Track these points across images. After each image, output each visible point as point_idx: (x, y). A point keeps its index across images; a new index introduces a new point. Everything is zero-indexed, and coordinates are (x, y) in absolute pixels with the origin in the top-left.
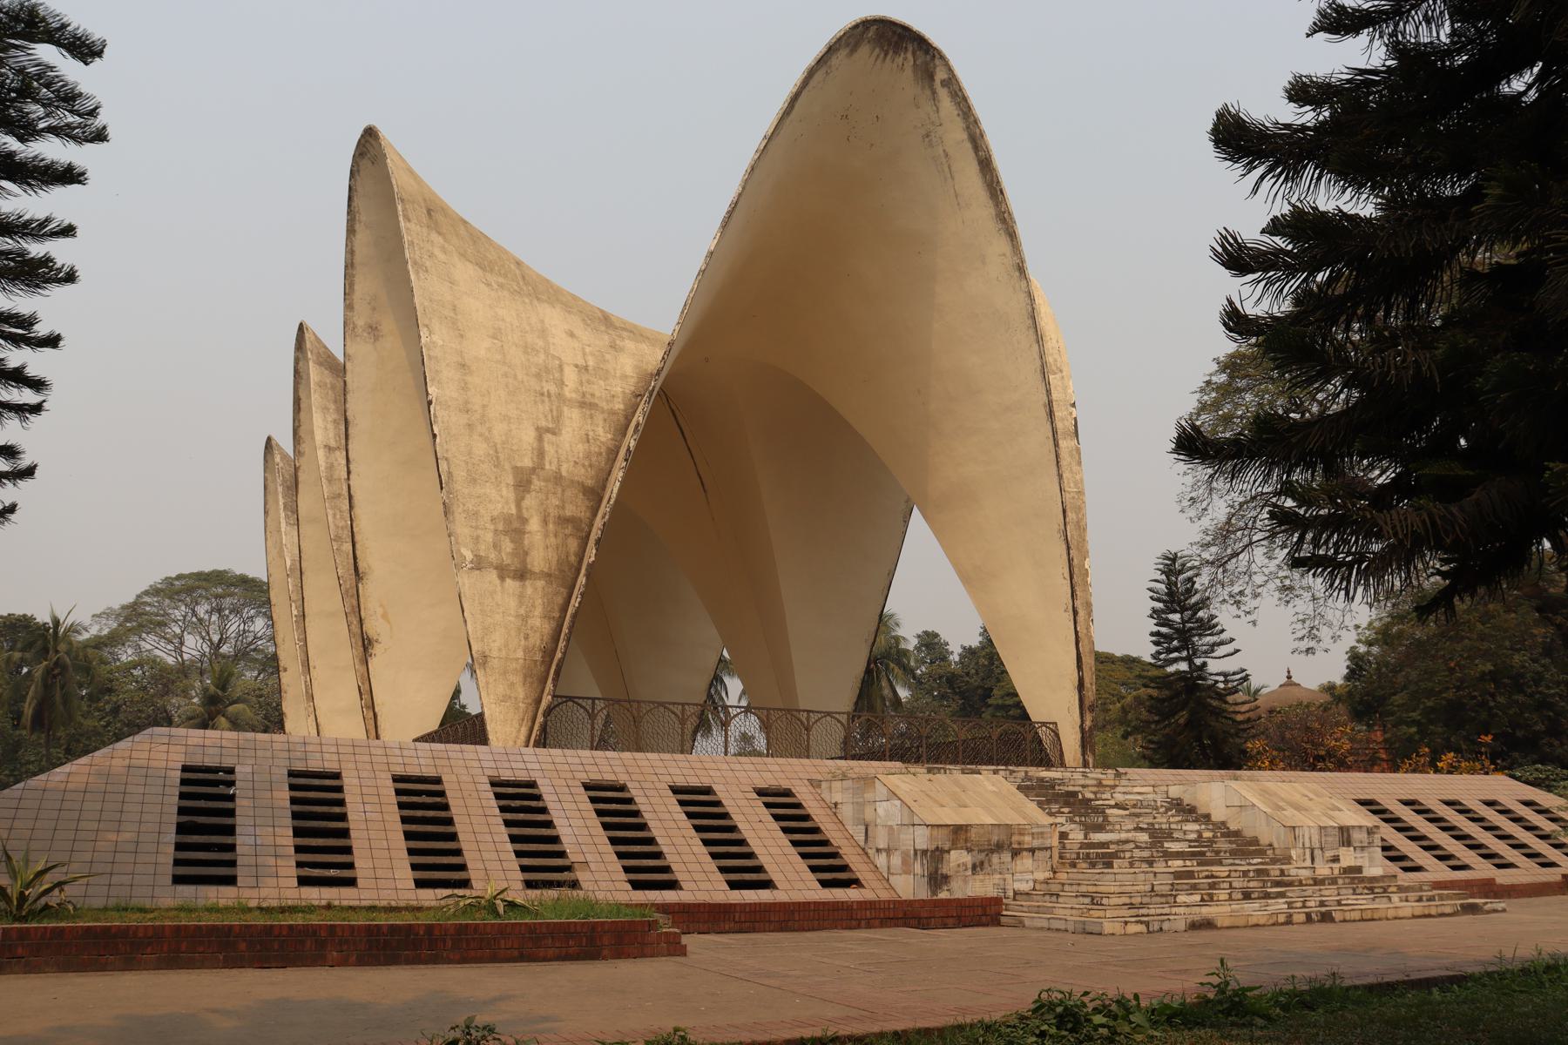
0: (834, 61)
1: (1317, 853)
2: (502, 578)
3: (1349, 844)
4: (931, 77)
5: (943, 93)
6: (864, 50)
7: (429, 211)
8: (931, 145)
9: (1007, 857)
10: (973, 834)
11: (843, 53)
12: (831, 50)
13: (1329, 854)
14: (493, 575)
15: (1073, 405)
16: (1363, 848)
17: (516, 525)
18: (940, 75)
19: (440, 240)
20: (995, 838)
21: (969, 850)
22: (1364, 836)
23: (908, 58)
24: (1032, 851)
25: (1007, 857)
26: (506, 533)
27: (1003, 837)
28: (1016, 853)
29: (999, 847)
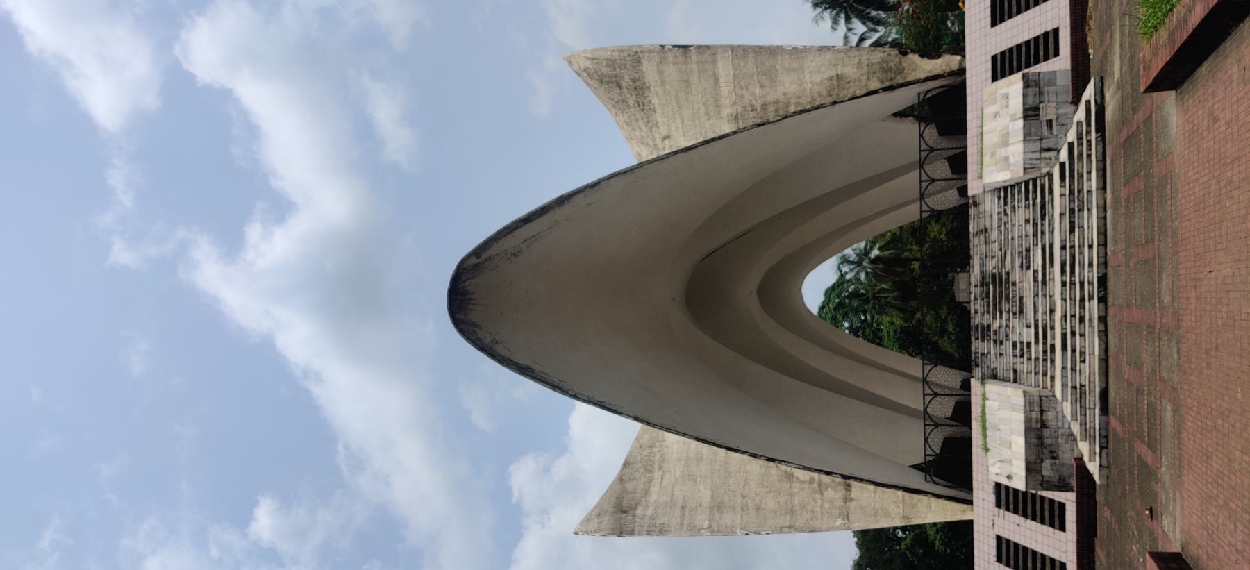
0: (488, 340)
1: (1045, 145)
2: (851, 500)
3: (1037, 109)
4: (476, 265)
5: (485, 256)
6: (474, 317)
7: (624, 512)
8: (520, 251)
9: (1047, 432)
10: (1032, 458)
11: (481, 334)
12: (483, 348)
13: (1045, 132)
14: (852, 505)
15: (663, 47)
16: (1041, 93)
17: (815, 485)
18: (474, 260)
19: (640, 508)
20: (1034, 441)
21: (1042, 461)
22: (1031, 91)
23: (470, 285)
24: (1042, 412)
25: (1047, 432)
26: (821, 493)
27: (1033, 434)
28: (1044, 425)
29: (1040, 438)
